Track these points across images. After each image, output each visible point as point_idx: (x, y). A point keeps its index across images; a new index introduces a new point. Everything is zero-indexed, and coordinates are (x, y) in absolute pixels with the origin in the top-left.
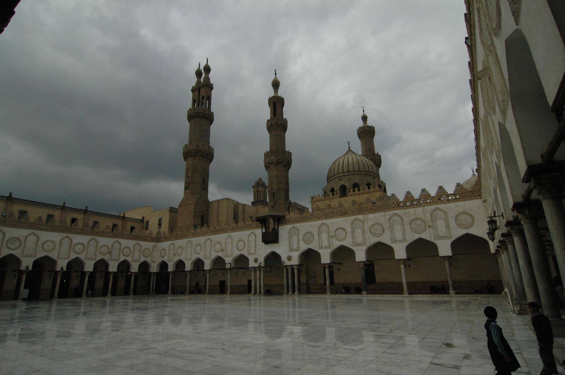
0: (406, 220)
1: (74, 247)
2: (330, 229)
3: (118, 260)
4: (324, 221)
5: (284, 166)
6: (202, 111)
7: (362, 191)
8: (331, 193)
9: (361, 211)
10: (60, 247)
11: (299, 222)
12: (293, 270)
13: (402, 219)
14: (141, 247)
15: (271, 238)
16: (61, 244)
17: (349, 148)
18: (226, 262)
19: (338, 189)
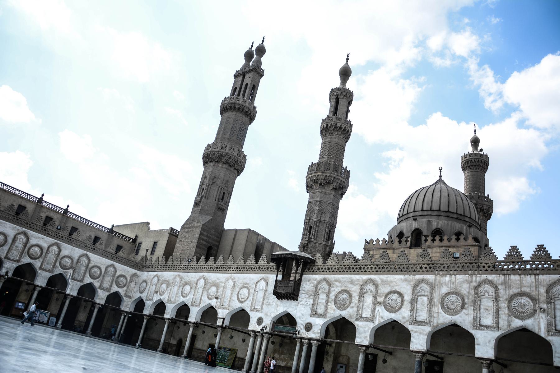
0: (504, 294)
1: (29, 249)
2: (379, 291)
3: (82, 281)
4: (373, 277)
5: (334, 189)
6: (241, 102)
7: (445, 242)
8: (398, 239)
9: (432, 268)
10: (12, 244)
12: (310, 346)
13: (497, 289)
14: (116, 271)
15: (287, 291)
16: (14, 240)
17: (441, 177)
18: (219, 315)
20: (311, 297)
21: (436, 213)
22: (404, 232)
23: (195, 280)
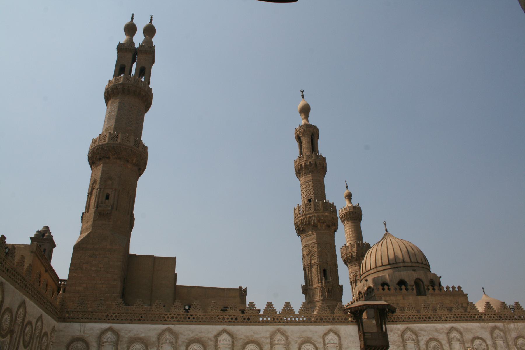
2: (464, 338)
11: (415, 322)
17: (386, 230)
19: (413, 283)
20: (400, 348)
21: (421, 265)
22: (407, 280)
23: (211, 336)
